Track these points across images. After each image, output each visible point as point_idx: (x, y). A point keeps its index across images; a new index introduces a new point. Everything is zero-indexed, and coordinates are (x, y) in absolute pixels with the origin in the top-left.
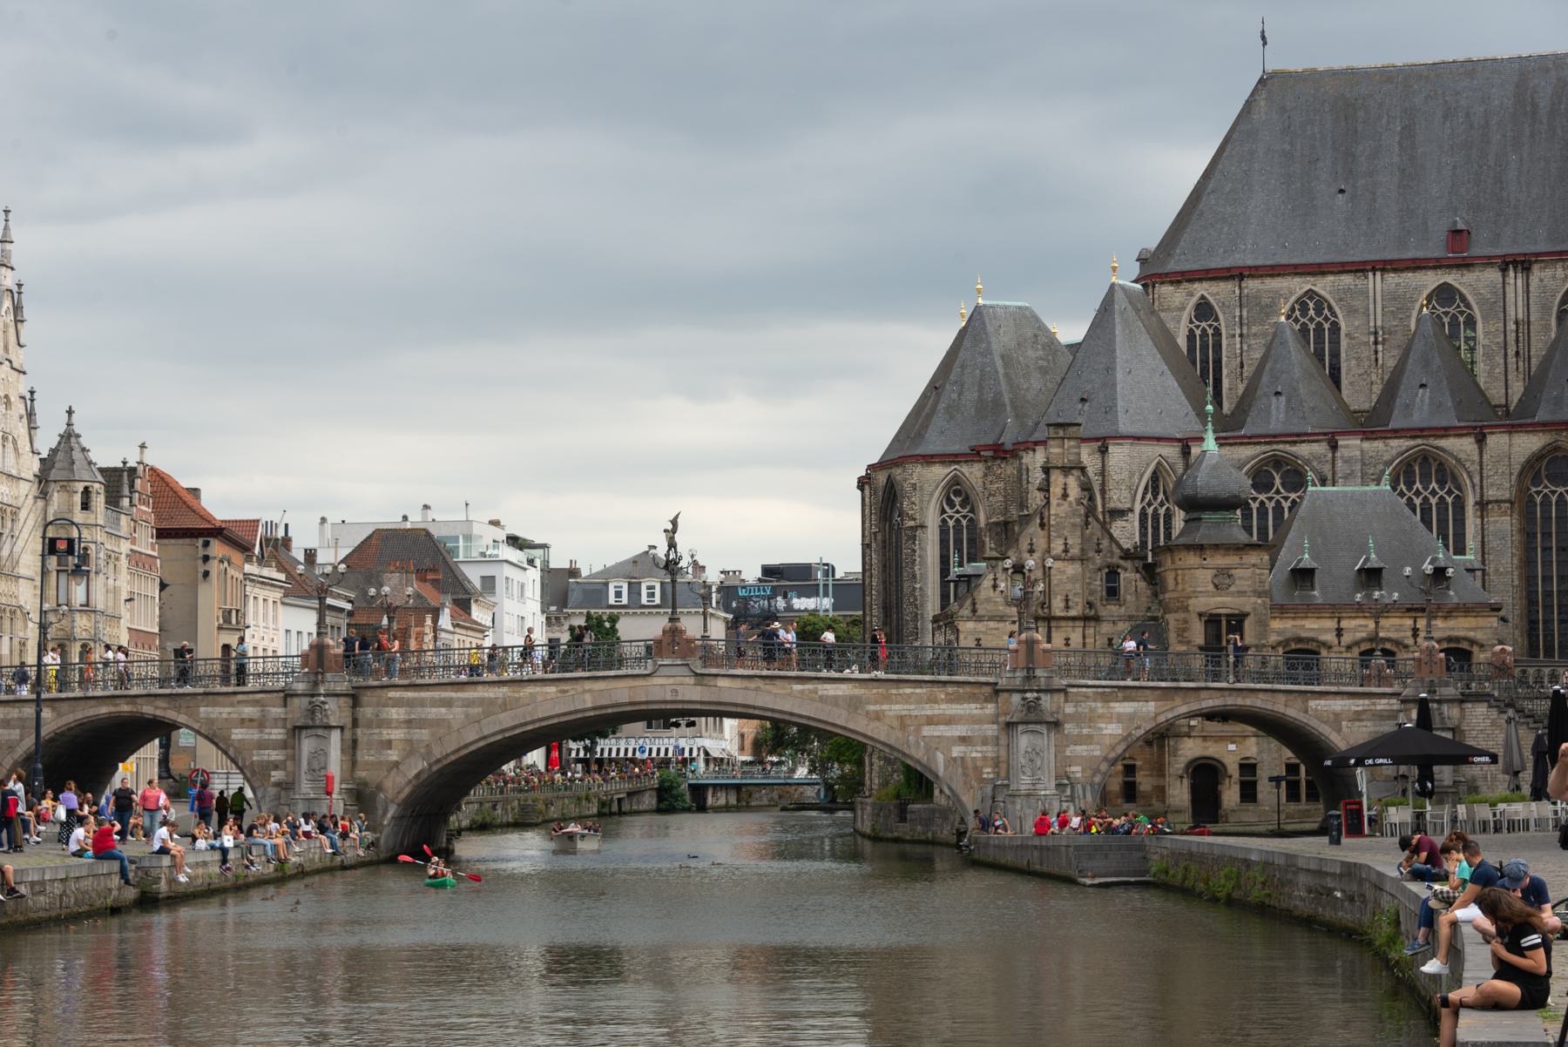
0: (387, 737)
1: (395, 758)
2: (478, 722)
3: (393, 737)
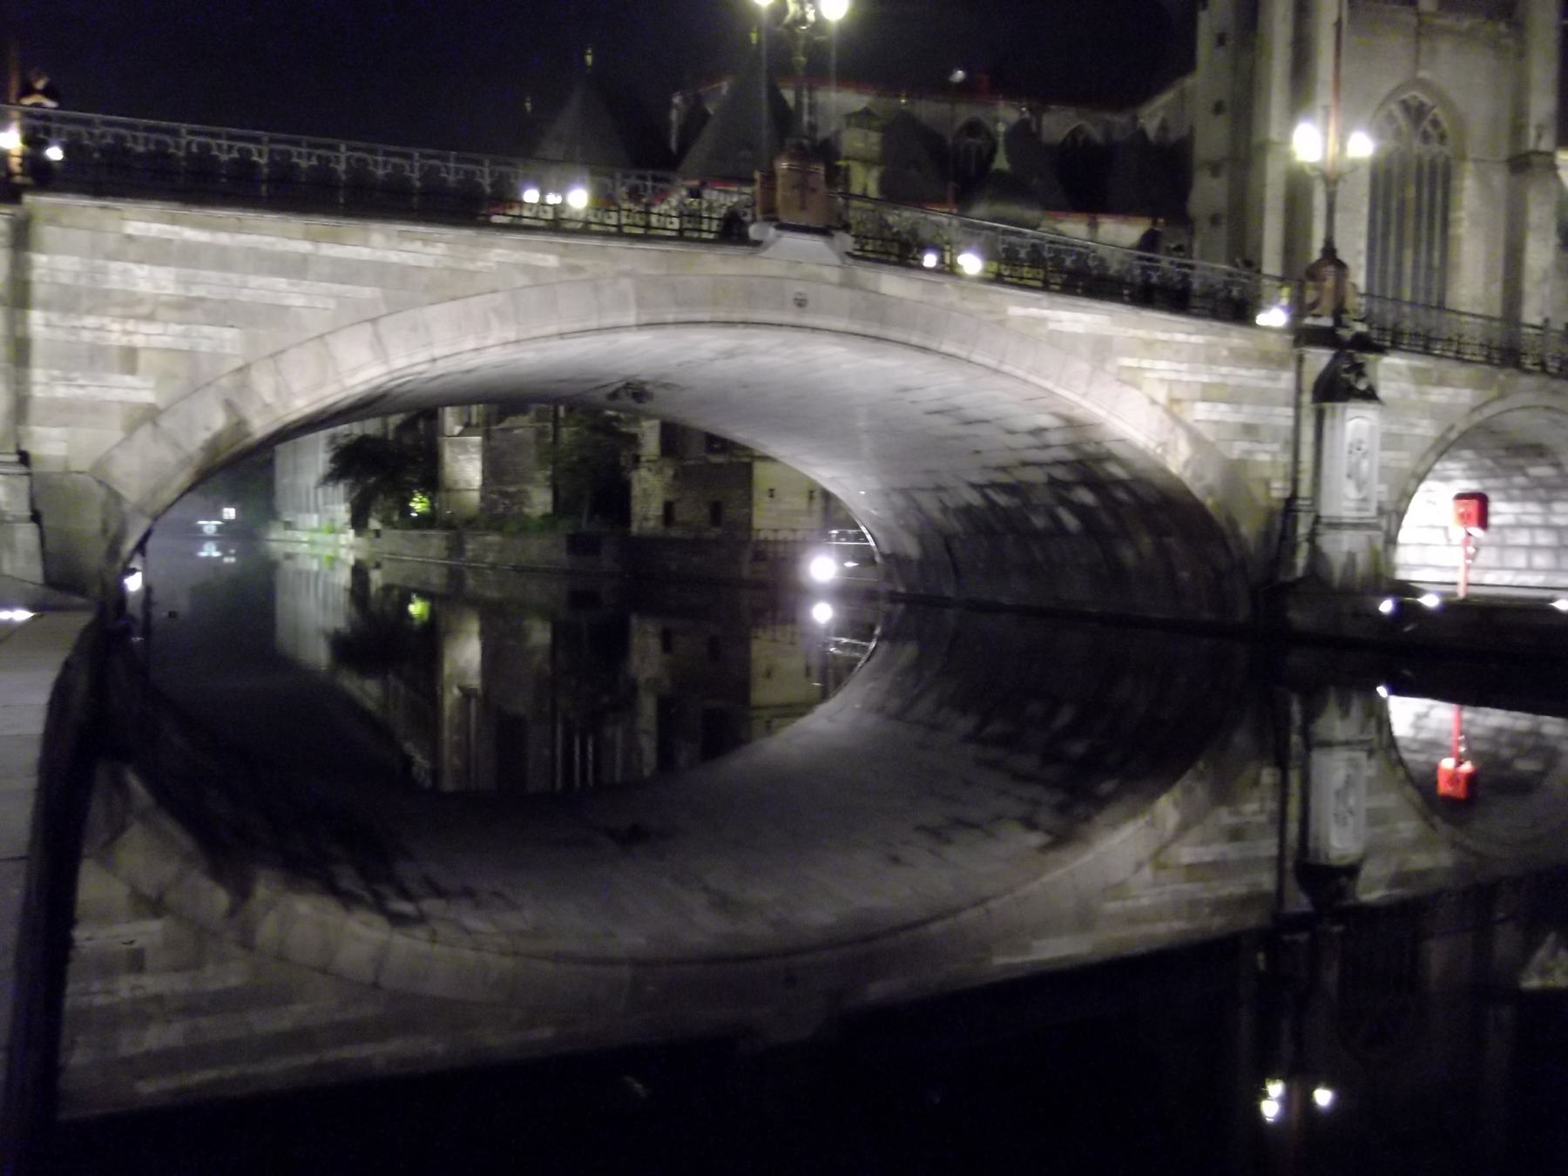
0: (124, 341)
1: (148, 397)
2: (373, 321)
3: (139, 341)
